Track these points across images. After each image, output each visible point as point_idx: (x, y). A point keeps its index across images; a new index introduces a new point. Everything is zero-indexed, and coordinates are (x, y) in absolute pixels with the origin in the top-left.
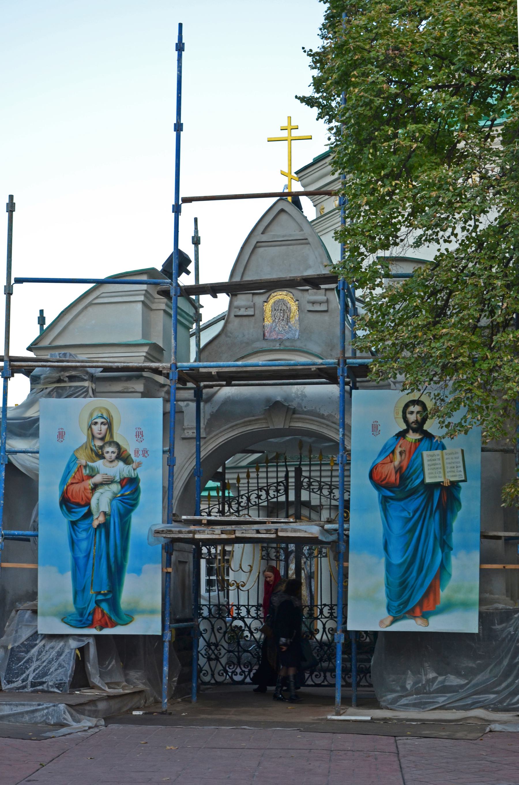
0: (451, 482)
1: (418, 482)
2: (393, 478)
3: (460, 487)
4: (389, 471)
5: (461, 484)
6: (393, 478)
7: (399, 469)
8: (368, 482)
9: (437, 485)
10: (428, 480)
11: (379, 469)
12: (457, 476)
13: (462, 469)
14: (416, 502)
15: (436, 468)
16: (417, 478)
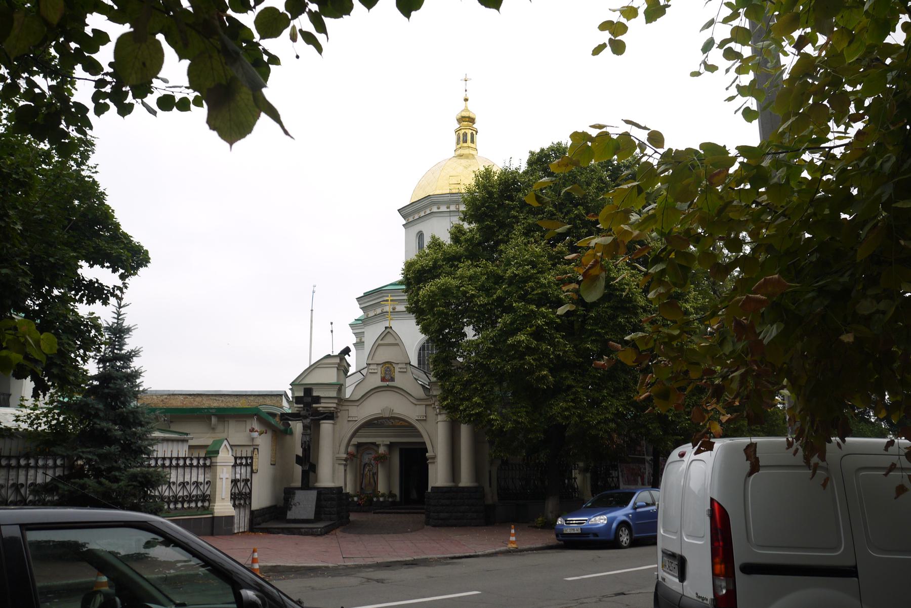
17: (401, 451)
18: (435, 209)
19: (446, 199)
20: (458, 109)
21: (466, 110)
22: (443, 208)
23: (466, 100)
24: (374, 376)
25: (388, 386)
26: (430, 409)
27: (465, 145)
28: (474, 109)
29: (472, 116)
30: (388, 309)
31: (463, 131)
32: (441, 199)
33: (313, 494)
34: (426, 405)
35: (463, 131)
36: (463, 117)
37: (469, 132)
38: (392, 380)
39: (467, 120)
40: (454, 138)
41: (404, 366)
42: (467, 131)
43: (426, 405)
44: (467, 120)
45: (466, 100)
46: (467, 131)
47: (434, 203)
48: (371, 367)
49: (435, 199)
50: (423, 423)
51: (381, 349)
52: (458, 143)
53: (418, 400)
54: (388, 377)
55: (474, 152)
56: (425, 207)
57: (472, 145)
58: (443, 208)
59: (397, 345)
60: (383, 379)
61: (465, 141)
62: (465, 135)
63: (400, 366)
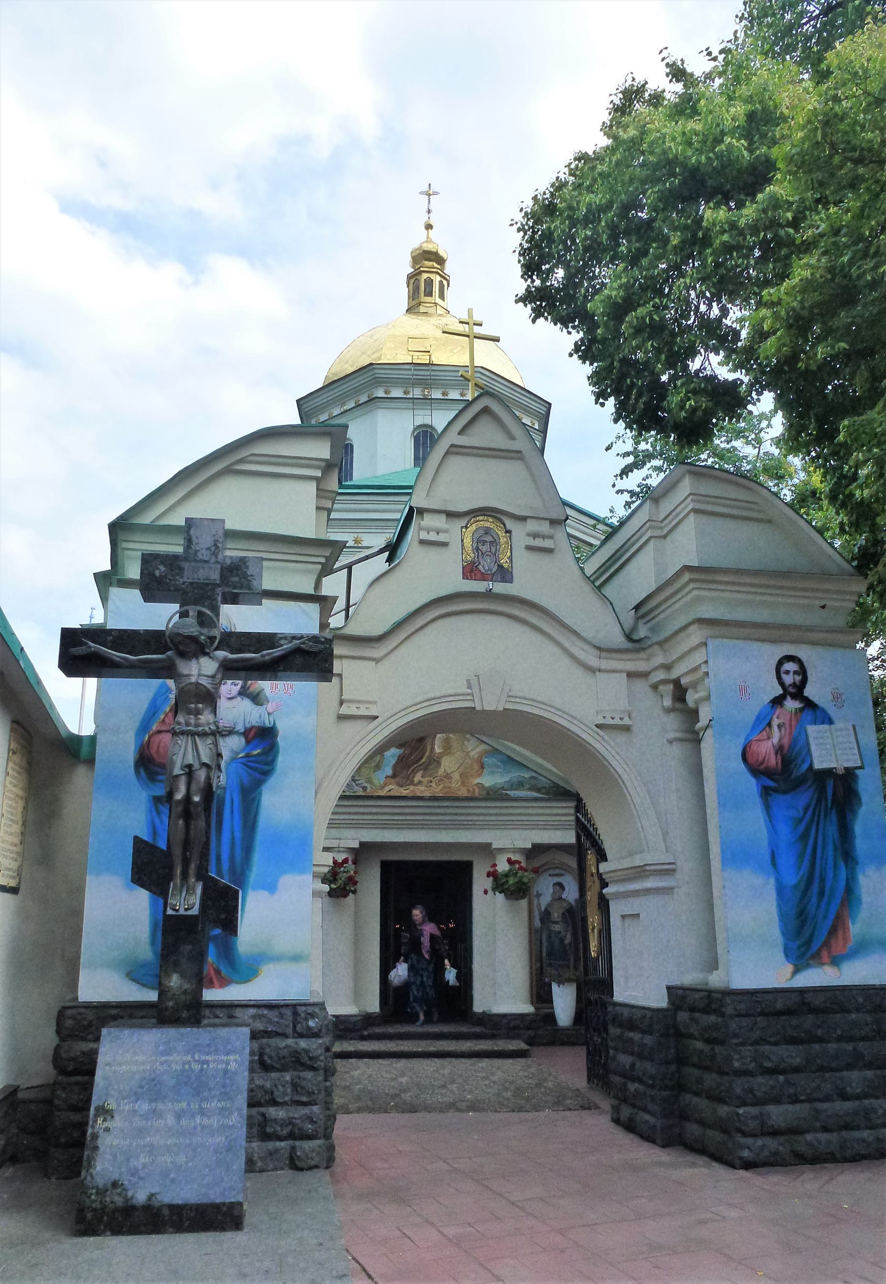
0: (846, 769)
1: (805, 766)
2: (773, 761)
3: (856, 776)
4: (766, 750)
5: (858, 772)
6: (773, 761)
7: (779, 749)
8: (742, 766)
9: (829, 772)
10: (817, 766)
11: (754, 747)
12: (851, 760)
13: (856, 751)
14: (803, 798)
15: (829, 749)
16: (803, 761)
17: (387, 868)
18: (380, 393)
19: (404, 374)
20: (417, 239)
22: (397, 393)
24: (433, 554)
25: (489, 595)
26: (642, 687)
27: (428, 299)
31: (425, 276)
32: (394, 374)
33: (229, 1054)
34: (631, 675)
35: (425, 276)
36: (425, 252)
37: (437, 279)
38: (505, 575)
41: (544, 528)
43: (631, 675)
46: (432, 276)
47: (377, 382)
48: (428, 520)
49: (380, 373)
50: (622, 738)
51: (455, 461)
53: (602, 650)
54: (486, 564)
56: (357, 391)
58: (397, 393)
59: (516, 455)
60: (470, 571)
61: (429, 293)
62: (429, 283)
63: (532, 526)
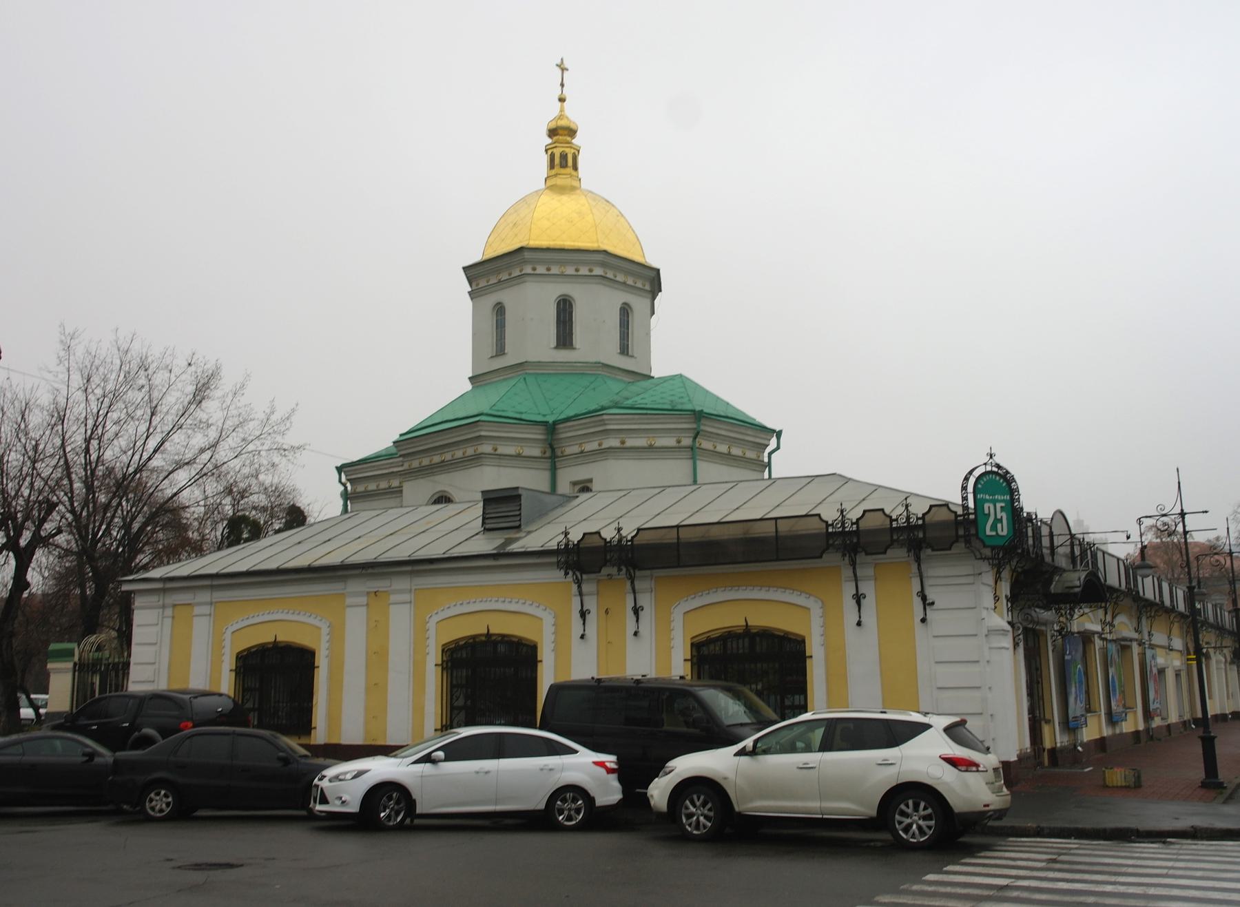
20: (548, 114)
21: (561, 116)
23: (562, 100)
27: (563, 171)
28: (574, 114)
29: (573, 126)
30: (486, 448)
37: (570, 152)
39: (561, 132)
40: (545, 159)
42: (567, 150)
44: (561, 132)
45: (562, 100)
52: (552, 165)
55: (575, 184)
57: (574, 173)
61: (564, 164)
62: (564, 157)
